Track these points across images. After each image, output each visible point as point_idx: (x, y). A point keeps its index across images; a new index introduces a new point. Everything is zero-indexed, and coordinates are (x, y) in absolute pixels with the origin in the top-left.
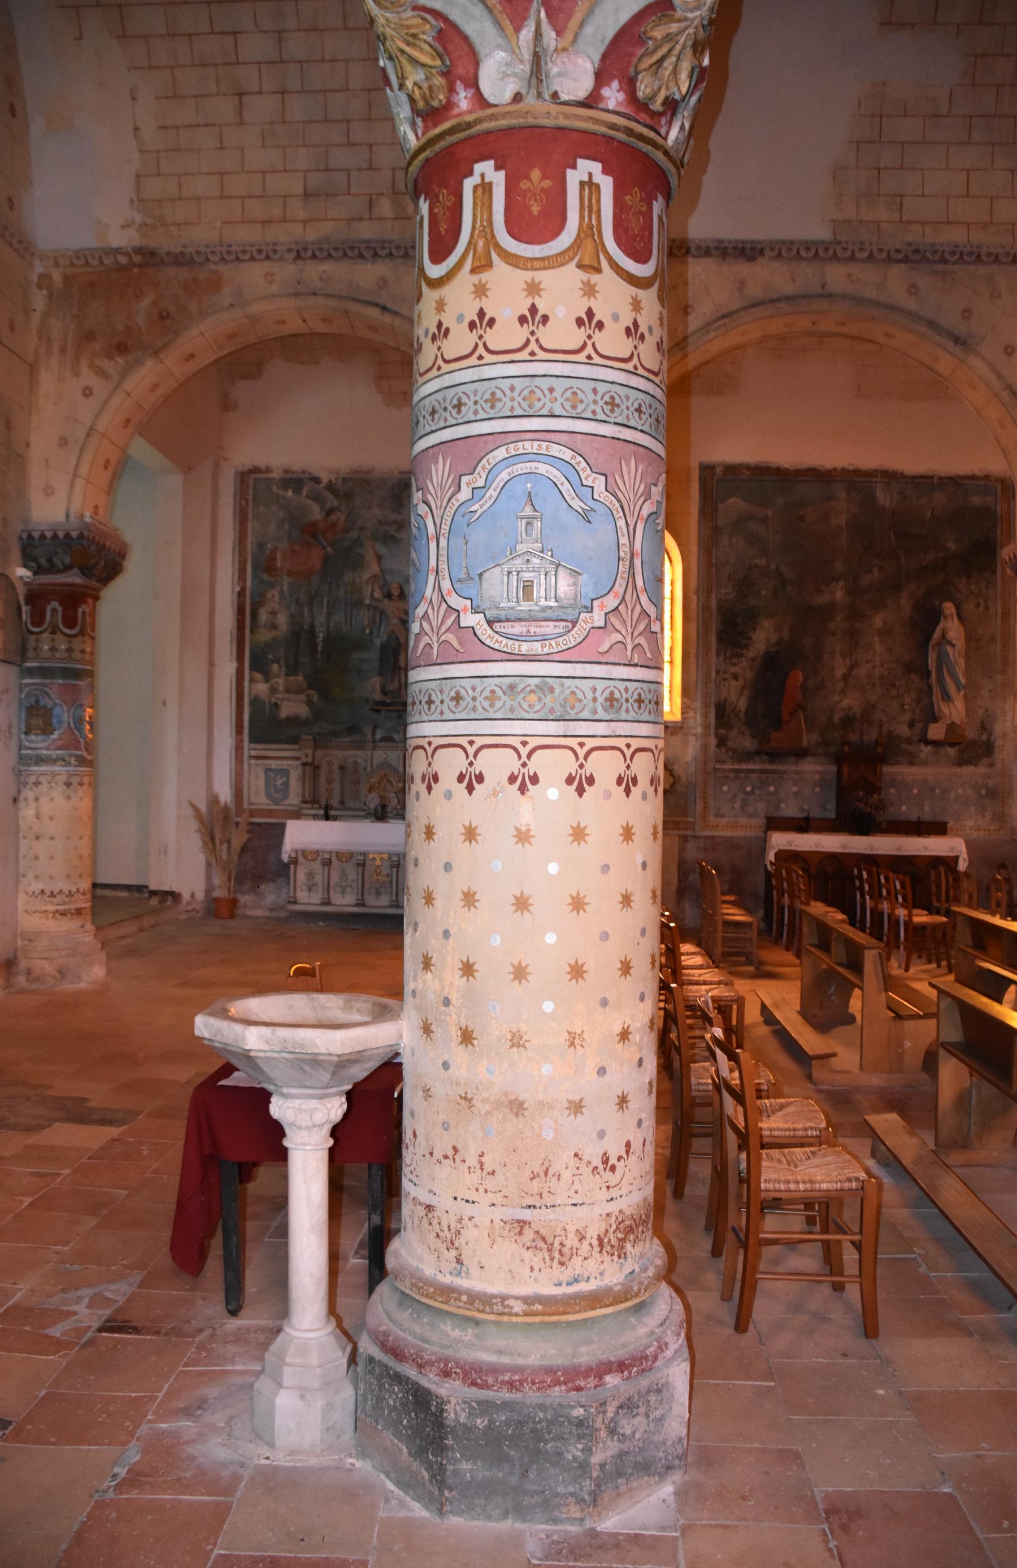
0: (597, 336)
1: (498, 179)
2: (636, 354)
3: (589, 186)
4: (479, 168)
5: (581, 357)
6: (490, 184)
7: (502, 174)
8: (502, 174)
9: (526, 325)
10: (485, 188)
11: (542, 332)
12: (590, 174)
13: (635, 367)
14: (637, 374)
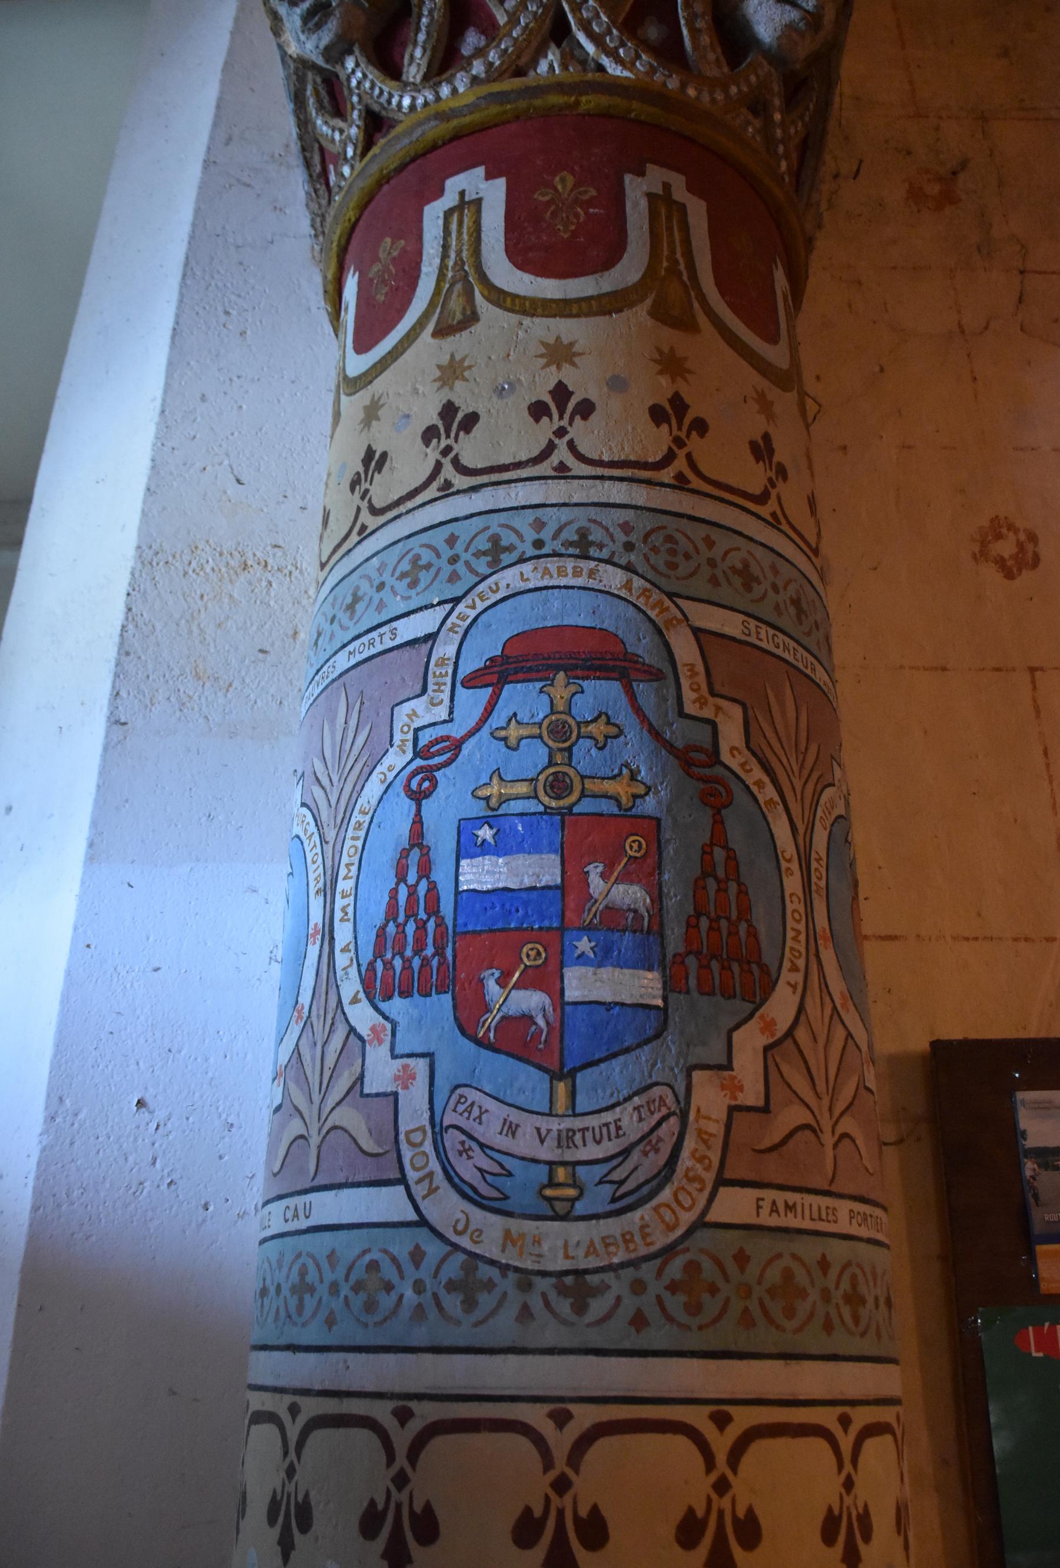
0: (695, 443)
1: (494, 195)
2: (773, 493)
3: (661, 203)
4: (454, 185)
5: (667, 475)
6: (478, 202)
7: (500, 184)
8: (500, 184)
9: (545, 419)
10: (469, 206)
11: (578, 430)
12: (667, 186)
13: (774, 515)
14: (779, 529)
